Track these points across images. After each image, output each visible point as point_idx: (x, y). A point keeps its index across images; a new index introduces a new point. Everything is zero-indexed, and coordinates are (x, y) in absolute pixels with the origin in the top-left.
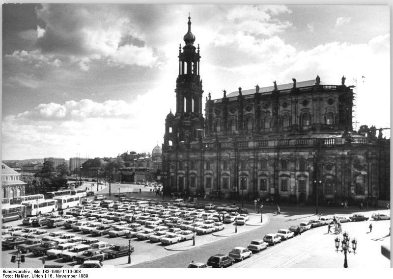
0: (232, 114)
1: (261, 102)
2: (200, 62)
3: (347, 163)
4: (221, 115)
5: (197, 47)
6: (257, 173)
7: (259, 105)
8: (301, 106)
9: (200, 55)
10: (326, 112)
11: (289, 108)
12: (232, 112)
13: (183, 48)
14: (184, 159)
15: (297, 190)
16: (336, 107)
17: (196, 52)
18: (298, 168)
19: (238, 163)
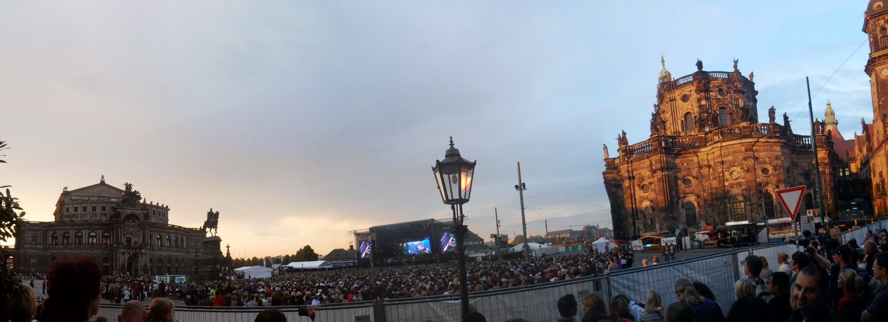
10: (682, 113)
16: (694, 104)
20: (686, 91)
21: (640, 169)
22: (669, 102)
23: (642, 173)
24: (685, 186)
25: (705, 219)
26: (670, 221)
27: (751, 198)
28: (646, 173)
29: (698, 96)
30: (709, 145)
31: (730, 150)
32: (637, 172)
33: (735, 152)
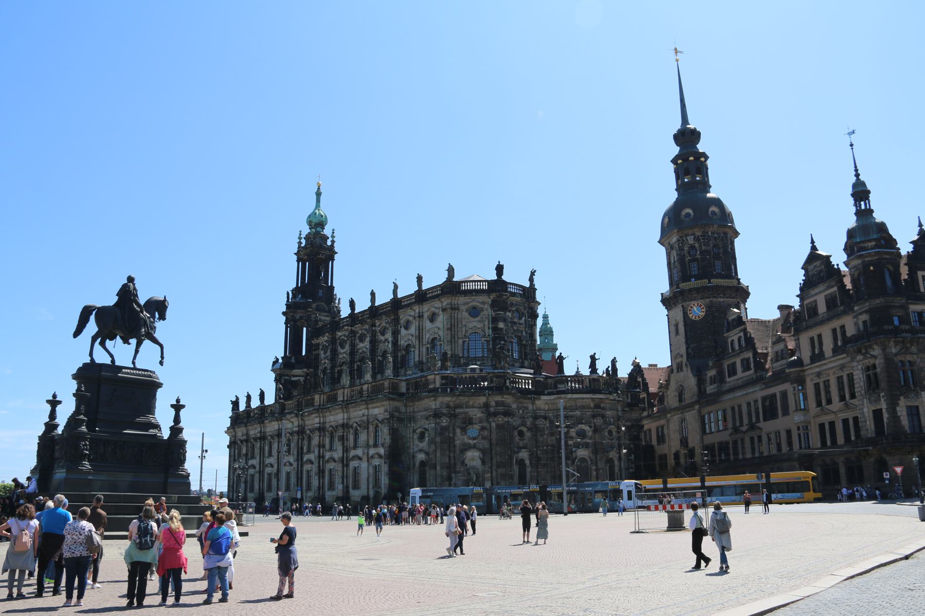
0: (342, 351)
1: (377, 324)
2: (334, 261)
3: (444, 424)
4: (328, 353)
5: (329, 236)
6: (323, 457)
7: (374, 328)
8: (428, 324)
9: (336, 249)
10: (466, 331)
11: (413, 330)
12: (341, 348)
13: (304, 238)
14: (242, 438)
15: (371, 486)
16: (486, 323)
17: (329, 243)
18: (371, 442)
19: (303, 439)
20: (477, 301)
21: (467, 407)
22: (449, 310)
23: (470, 413)
24: (519, 438)
25: (536, 481)
26: (509, 480)
27: (599, 462)
28: (477, 414)
29: (493, 314)
30: (549, 394)
31: (578, 404)
32: (462, 410)
33: (583, 407)
